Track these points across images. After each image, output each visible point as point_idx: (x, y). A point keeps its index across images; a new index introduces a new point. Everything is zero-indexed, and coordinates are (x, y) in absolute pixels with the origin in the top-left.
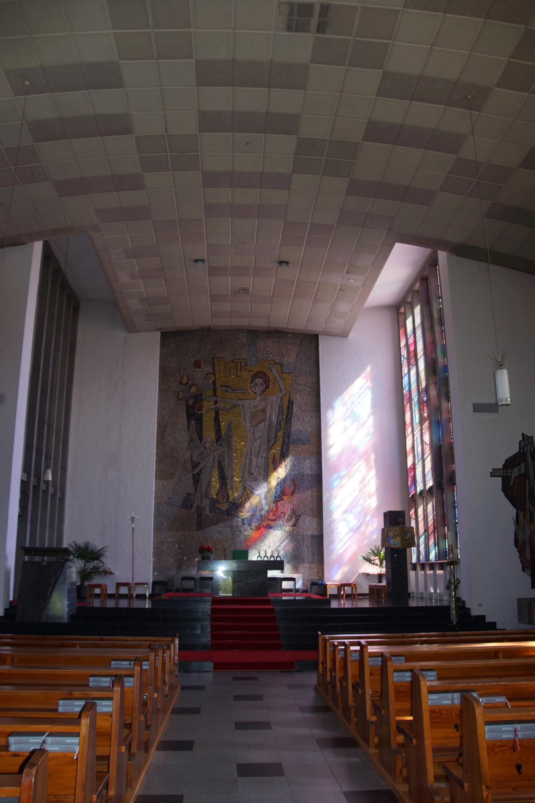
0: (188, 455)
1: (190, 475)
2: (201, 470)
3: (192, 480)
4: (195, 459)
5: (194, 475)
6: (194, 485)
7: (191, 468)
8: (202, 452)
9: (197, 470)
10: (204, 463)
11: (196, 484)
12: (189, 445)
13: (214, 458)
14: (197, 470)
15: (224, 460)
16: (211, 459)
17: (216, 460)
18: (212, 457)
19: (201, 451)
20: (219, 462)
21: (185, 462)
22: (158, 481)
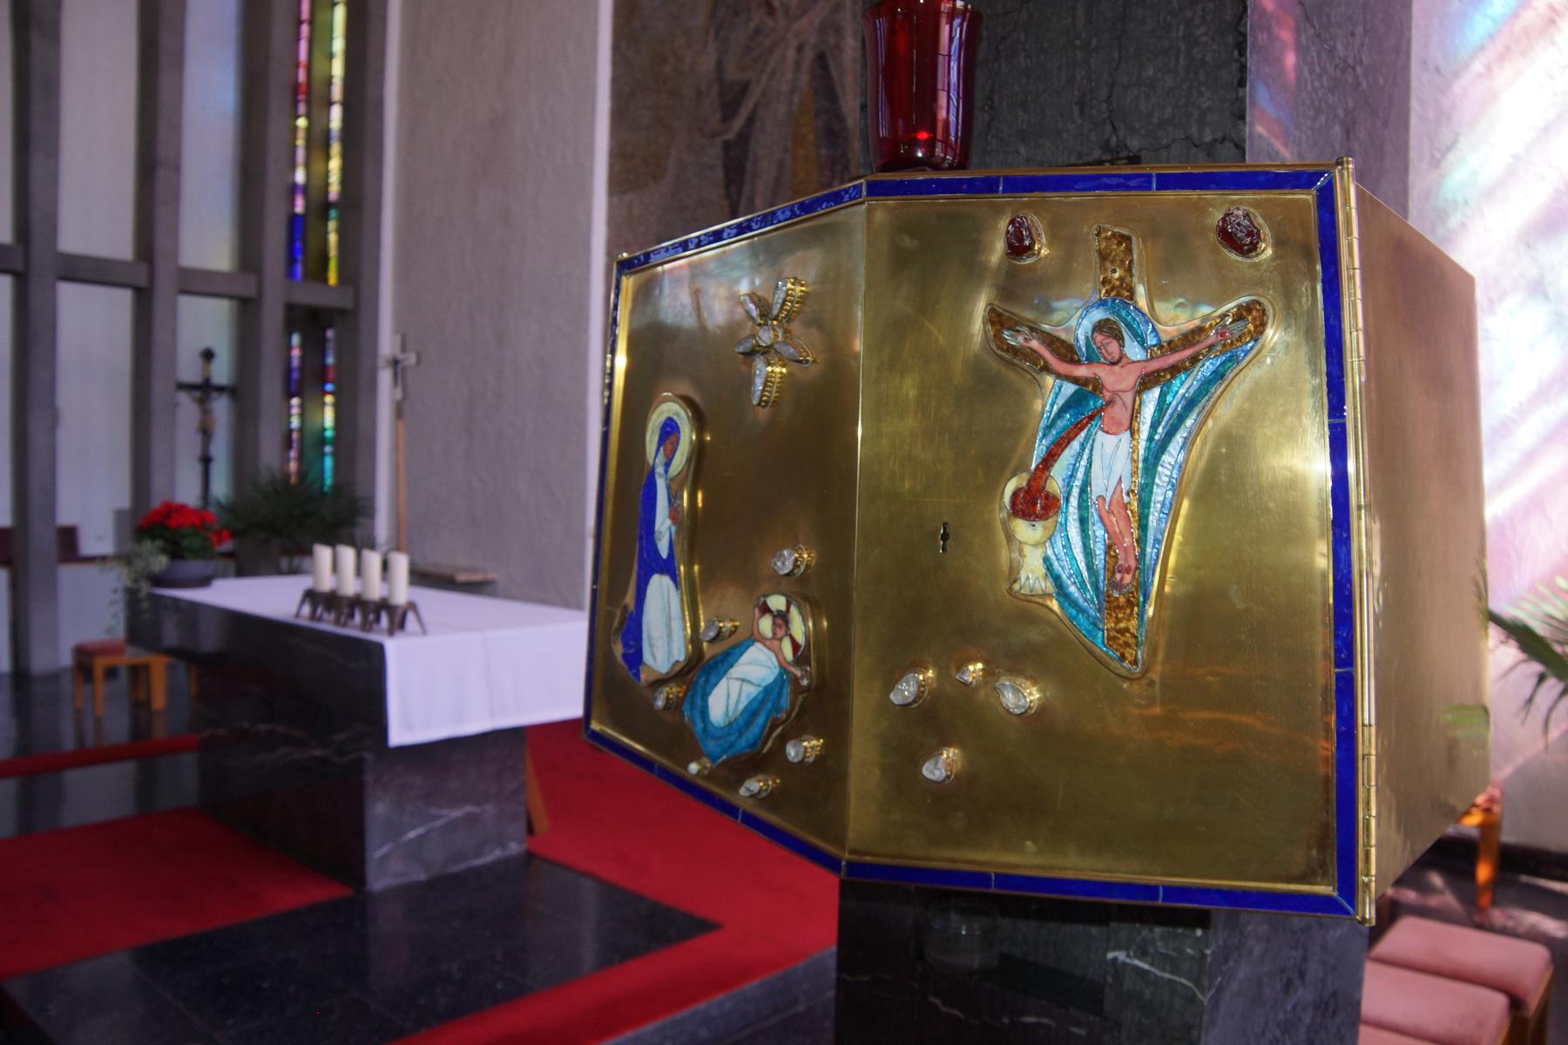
0: (707, 63)
1: (714, 153)
2: (751, 119)
3: (720, 173)
4: (732, 73)
5: (727, 146)
6: (728, 195)
7: (718, 116)
8: (758, 31)
9: (738, 123)
10: (764, 79)
11: (733, 189)
12: (712, 15)
13: (800, 48)
14: (738, 123)
15: (838, 47)
16: (791, 54)
17: (809, 55)
18: (794, 43)
19: (752, 25)
20: (821, 58)
21: (699, 94)
22: (615, 200)
